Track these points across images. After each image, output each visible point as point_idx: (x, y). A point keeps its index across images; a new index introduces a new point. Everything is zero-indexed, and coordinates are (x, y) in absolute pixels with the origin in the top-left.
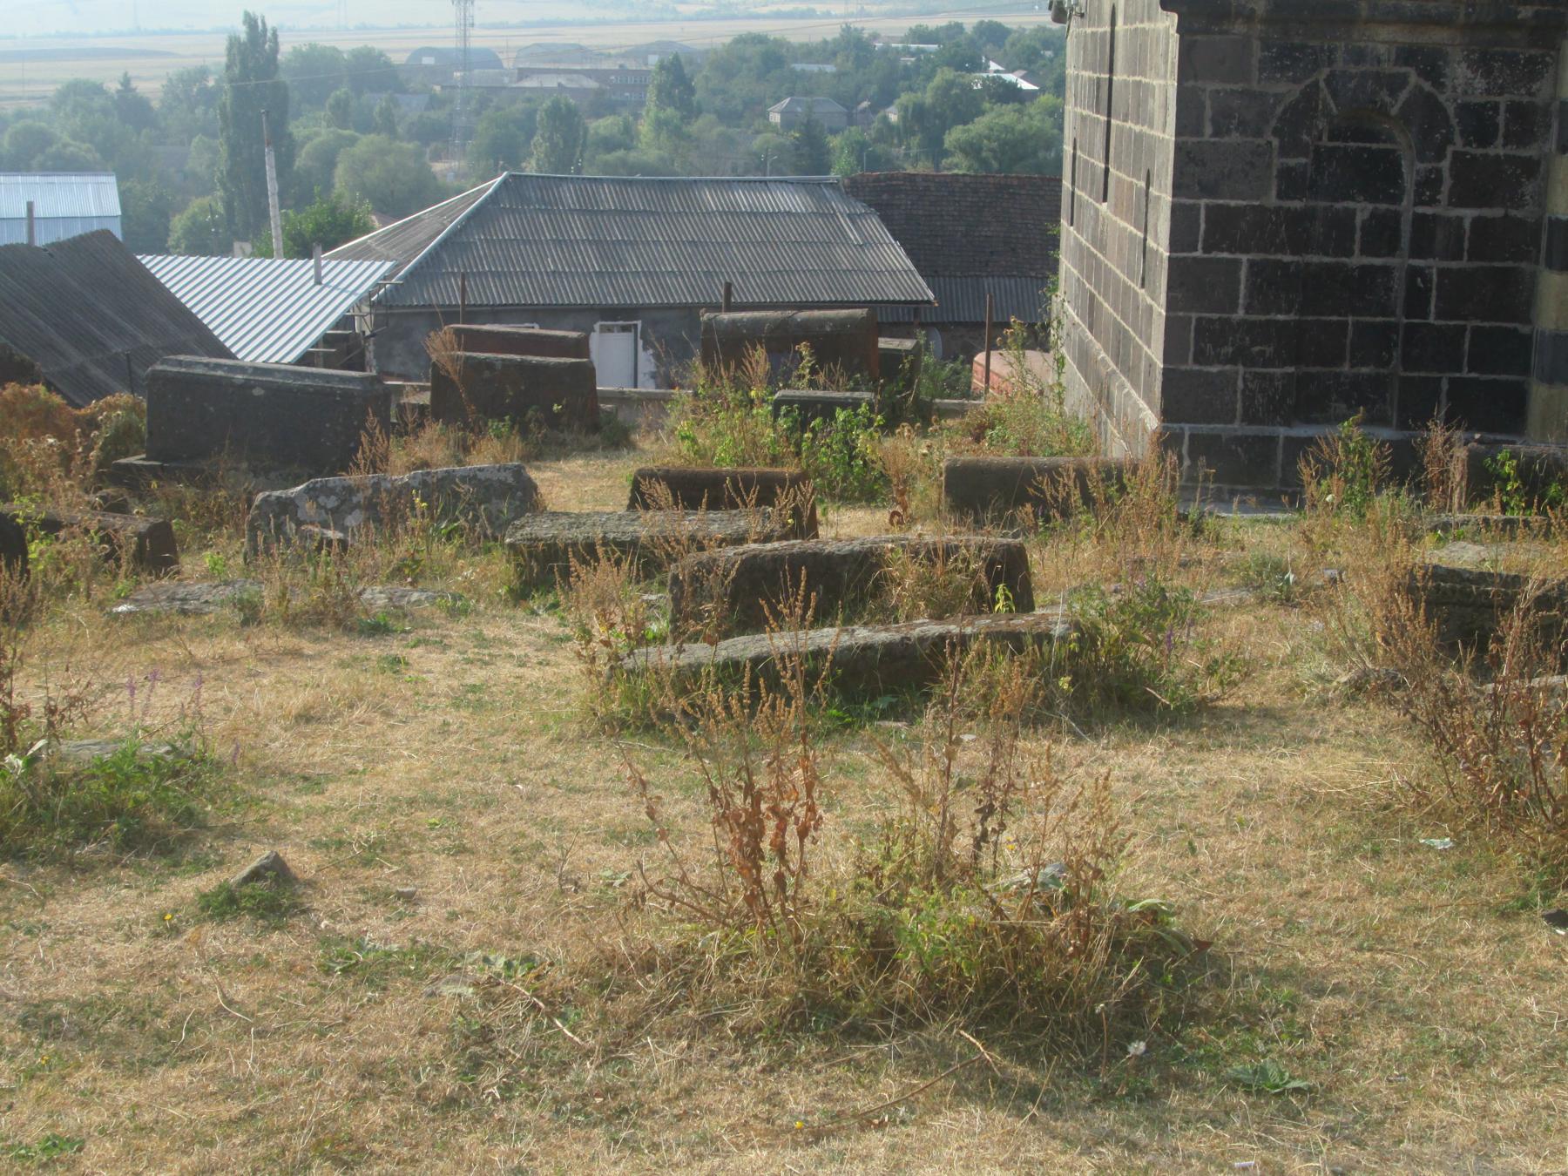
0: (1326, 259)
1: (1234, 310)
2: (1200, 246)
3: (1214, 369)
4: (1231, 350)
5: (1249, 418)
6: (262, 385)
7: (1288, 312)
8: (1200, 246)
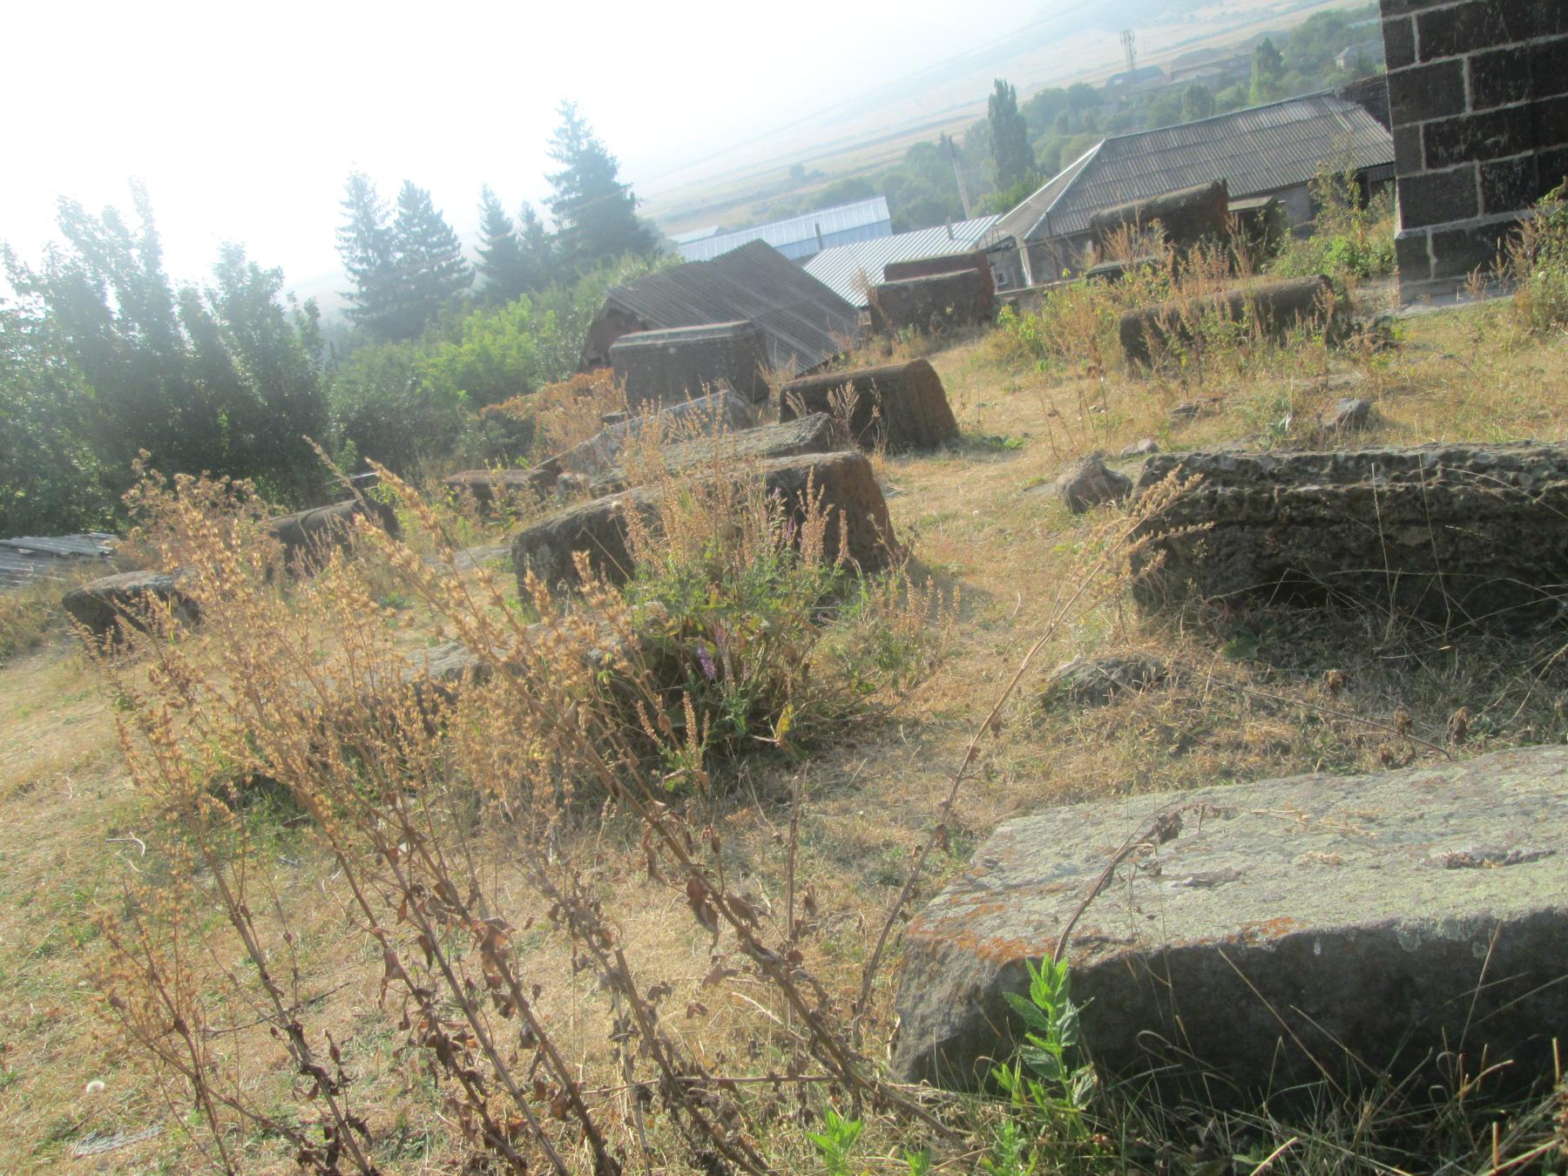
0: (1553, 38)
1: (1461, 108)
2: (1417, 57)
3: (1450, 169)
4: (1463, 148)
5: (1492, 207)
6: (674, 345)
7: (1518, 98)
8: (1417, 57)
